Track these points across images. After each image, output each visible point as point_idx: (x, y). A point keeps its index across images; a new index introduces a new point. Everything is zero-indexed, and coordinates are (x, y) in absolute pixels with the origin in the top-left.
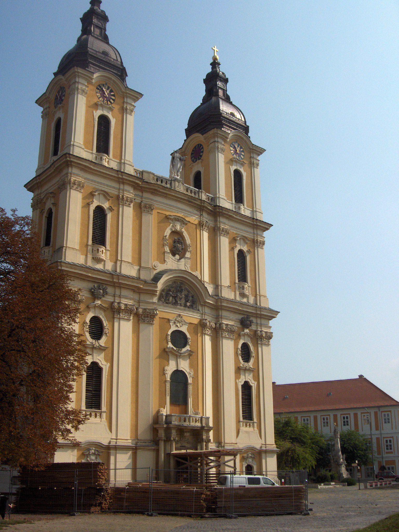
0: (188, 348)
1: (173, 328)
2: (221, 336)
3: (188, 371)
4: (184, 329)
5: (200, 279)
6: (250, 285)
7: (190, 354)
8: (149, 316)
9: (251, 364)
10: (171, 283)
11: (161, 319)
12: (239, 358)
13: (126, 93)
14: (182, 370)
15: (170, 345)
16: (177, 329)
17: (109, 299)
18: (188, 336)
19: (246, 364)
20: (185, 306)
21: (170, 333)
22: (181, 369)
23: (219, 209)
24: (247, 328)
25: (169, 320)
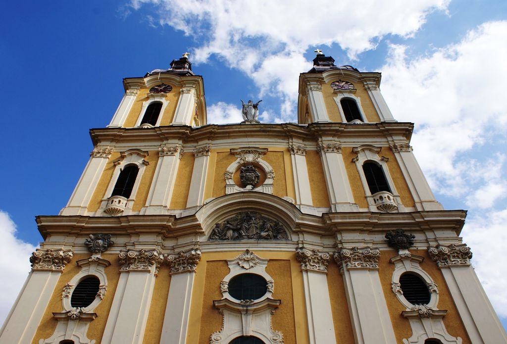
0: (268, 295)
1: (235, 271)
2: (345, 269)
3: (269, 335)
4: (260, 270)
5: (293, 203)
6: (396, 192)
7: (273, 307)
8: (186, 262)
9: (434, 303)
10: (234, 216)
11: (211, 263)
12: (398, 301)
13: (183, 81)
14: (251, 336)
15: (227, 296)
16: (243, 271)
17: (115, 251)
18: (268, 278)
19: (423, 308)
20: (260, 237)
21: (227, 279)
22: (251, 334)
23: (314, 127)
24: (404, 248)
25: (226, 262)
